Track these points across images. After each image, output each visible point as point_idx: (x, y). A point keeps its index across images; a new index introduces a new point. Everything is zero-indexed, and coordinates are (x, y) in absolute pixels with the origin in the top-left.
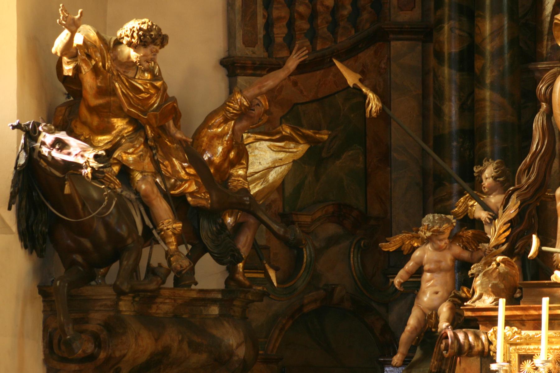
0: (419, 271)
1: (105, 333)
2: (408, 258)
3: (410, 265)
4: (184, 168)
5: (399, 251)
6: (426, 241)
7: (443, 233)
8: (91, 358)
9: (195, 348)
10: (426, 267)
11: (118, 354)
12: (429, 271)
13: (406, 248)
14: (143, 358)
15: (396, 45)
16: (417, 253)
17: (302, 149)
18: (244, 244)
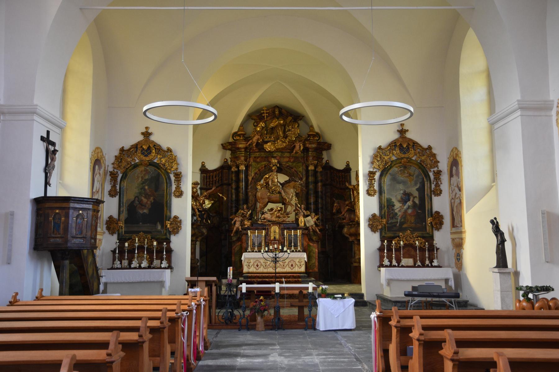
0: (236, 221)
18: (205, 216)
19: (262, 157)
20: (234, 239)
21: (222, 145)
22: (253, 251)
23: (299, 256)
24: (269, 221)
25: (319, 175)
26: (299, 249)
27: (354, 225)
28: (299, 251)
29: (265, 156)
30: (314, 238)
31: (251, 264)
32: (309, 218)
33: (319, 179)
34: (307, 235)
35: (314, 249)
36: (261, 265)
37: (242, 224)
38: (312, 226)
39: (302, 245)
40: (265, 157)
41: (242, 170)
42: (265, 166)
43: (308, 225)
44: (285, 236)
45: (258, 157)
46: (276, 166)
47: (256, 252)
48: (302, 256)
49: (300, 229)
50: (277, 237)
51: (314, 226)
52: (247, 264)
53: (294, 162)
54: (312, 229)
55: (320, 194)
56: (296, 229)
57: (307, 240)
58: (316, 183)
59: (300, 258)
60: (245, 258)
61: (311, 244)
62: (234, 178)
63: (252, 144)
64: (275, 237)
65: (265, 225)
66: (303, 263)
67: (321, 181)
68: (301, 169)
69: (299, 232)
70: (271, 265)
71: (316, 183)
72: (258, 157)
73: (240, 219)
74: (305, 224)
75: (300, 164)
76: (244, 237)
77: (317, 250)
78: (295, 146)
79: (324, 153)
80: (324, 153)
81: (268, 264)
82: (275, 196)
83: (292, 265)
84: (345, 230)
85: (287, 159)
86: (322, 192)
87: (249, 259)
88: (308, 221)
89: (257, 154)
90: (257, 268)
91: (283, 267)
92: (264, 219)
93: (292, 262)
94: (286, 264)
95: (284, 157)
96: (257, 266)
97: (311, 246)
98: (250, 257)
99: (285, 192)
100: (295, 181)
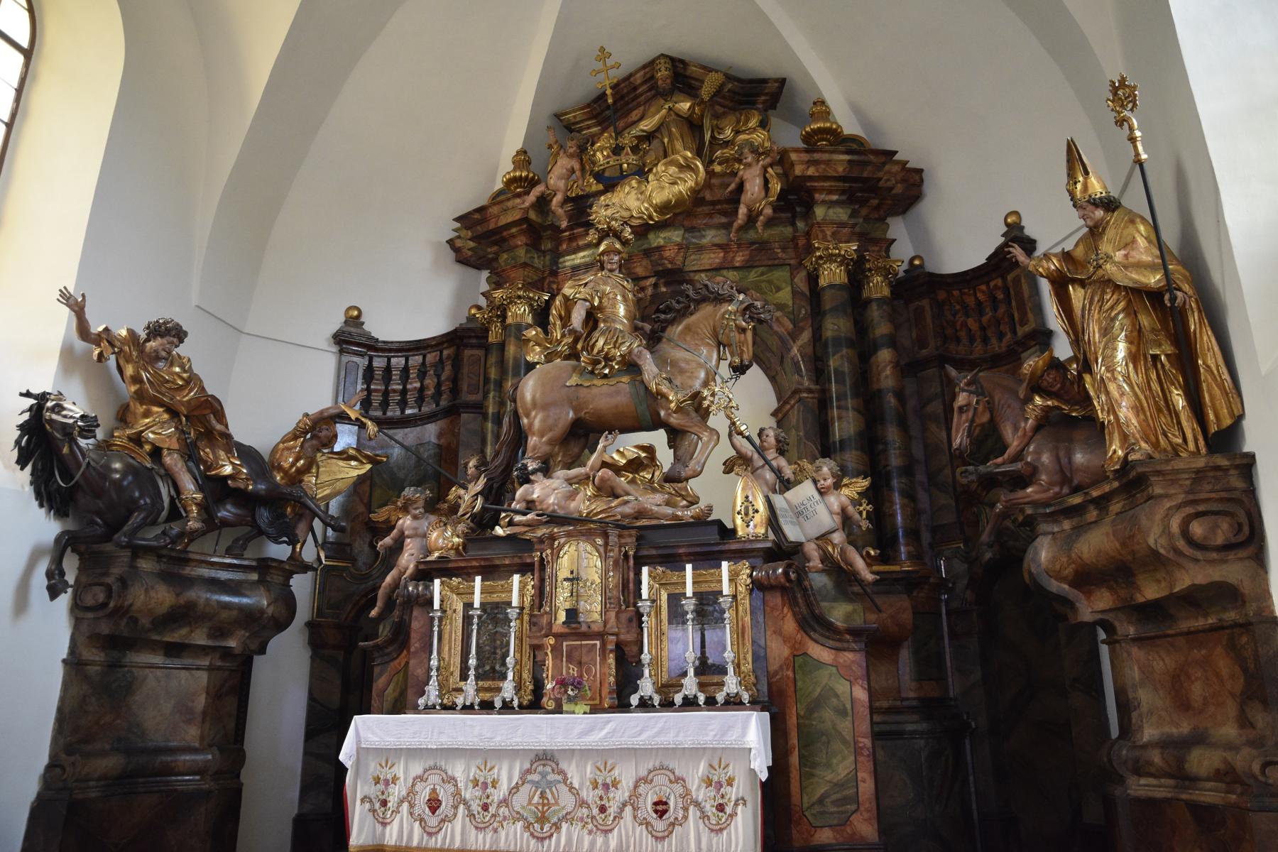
2: (393, 527)
5: (387, 521)
6: (405, 509)
7: (415, 502)
11: (126, 603)
13: (393, 518)
14: (163, 609)
15: (464, 416)
16: (401, 522)
17: (369, 466)
20: (384, 631)
21: (450, 242)
24: (555, 519)
25: (875, 313)
26: (731, 684)
27: (1102, 503)
30: (839, 613)
31: (396, 792)
32: (805, 492)
33: (882, 329)
34: (782, 589)
35: (842, 687)
36: (459, 800)
38: (824, 537)
43: (792, 533)
44: (644, 606)
46: (618, 235)
48: (731, 739)
50: (592, 609)
51: (838, 537)
53: (747, 267)
54: (826, 557)
55: (891, 400)
56: (707, 558)
57: (790, 625)
58: (863, 346)
59: (720, 757)
60: (362, 752)
61: (819, 652)
63: (543, 203)
65: (528, 545)
67: (892, 342)
68: (785, 295)
69: (729, 578)
70: (519, 801)
71: (863, 346)
74: (773, 521)
75: (781, 275)
76: (416, 625)
77: (861, 694)
79: (897, 228)
80: (897, 228)
82: (609, 395)
83: (661, 808)
84: (1043, 553)
85: (715, 258)
86: (900, 395)
87: (389, 755)
88: (799, 513)
90: (433, 821)
92: (530, 505)
93: (660, 779)
94: (621, 794)
95: (700, 249)
97: (819, 664)
98: (390, 741)
99: (661, 362)
100: (719, 299)
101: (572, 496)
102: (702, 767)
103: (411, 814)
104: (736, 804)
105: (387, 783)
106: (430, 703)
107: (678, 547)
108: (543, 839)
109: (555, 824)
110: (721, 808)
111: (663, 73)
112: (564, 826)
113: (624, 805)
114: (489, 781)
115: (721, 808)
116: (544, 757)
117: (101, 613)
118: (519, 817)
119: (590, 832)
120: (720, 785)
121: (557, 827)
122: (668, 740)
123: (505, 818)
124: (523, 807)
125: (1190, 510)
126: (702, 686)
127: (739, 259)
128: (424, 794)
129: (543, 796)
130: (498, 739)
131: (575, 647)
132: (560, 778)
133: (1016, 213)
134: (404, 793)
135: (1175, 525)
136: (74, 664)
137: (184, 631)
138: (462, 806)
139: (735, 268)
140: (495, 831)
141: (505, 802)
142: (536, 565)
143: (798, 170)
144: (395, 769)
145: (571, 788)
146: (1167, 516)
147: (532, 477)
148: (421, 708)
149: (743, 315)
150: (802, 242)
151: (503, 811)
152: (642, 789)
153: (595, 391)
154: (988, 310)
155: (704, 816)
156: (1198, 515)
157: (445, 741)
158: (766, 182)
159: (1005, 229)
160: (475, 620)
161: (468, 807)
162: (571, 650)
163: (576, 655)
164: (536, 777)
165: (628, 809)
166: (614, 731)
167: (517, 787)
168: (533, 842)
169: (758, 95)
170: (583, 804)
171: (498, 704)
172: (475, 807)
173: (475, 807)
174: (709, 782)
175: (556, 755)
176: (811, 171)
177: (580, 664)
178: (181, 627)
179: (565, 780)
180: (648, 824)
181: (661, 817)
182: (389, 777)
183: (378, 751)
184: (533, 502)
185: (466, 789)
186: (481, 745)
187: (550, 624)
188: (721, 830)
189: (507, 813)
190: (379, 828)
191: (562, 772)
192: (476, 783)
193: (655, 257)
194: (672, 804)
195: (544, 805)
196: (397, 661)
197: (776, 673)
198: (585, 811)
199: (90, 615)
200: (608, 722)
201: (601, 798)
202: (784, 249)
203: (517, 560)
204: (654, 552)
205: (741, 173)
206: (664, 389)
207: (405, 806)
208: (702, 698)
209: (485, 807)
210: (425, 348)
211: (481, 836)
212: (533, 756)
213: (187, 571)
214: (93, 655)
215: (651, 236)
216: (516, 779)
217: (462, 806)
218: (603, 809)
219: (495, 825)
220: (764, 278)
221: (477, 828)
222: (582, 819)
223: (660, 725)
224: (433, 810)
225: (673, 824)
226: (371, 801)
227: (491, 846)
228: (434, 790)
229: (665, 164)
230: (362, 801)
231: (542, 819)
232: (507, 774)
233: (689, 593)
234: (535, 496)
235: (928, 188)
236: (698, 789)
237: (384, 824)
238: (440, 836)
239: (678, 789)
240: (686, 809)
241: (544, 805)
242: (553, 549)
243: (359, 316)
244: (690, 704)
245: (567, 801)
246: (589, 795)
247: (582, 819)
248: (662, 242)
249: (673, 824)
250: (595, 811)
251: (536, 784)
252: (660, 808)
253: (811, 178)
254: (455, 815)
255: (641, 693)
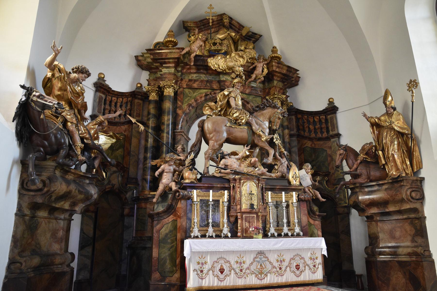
1: (48, 180)
2: (159, 168)
3: (160, 170)
4: (84, 130)
5: (156, 165)
6: (166, 162)
8: (40, 190)
9: (80, 192)
10: (166, 171)
11: (52, 189)
12: (166, 172)
13: (158, 165)
14: (62, 193)
16: (162, 167)
17: (114, 140)
19: (202, 81)
22: (204, 236)
23: (311, 245)
24: (236, 173)
28: (298, 235)
29: (206, 79)
31: (206, 268)
36: (231, 268)
37: (179, 177)
39: (300, 223)
40: (207, 81)
41: (169, 96)
42: (206, 95)
45: (195, 81)
47: (211, 237)
48: (317, 245)
49: (294, 190)
52: (198, 267)
53: (249, 94)
59: (313, 251)
60: (193, 253)
62: (152, 111)
64: (252, 205)
66: (320, 260)
70: (253, 268)
72: (195, 81)
73: (172, 168)
76: (181, 205)
78: (255, 68)
81: (245, 266)
83: (298, 267)
87: (202, 254)
89: (194, 76)
90: (222, 276)
91: (280, 271)
94: (285, 264)
96: (222, 271)
98: (204, 249)
101: (240, 166)
102: (309, 255)
103: (213, 274)
104: (319, 265)
105: (202, 264)
106: (196, 235)
107: (277, 186)
108: (262, 279)
109: (265, 274)
110: (314, 266)
111: (226, 21)
112: (269, 275)
113: (287, 267)
114: (242, 261)
115: (314, 266)
116: (261, 253)
117: (39, 193)
118: (253, 273)
119: (277, 276)
120: (314, 259)
121: (266, 275)
122: (300, 246)
123: (248, 274)
124: (254, 270)
125: (411, 190)
126: (289, 230)
127: (247, 91)
128: (219, 267)
129: (261, 265)
130: (245, 247)
131: (248, 217)
132: (266, 259)
133: (333, 99)
134: (210, 267)
135: (408, 193)
136: (20, 214)
137: (62, 203)
138: (232, 271)
139: (246, 94)
140: (245, 278)
141: (248, 268)
142: (232, 188)
143: (274, 68)
144: (205, 259)
145: (270, 262)
146: (407, 191)
147: (226, 157)
148: (192, 237)
149: (281, 114)
150: (267, 91)
151: (248, 271)
152: (292, 262)
153: (236, 129)
154: (318, 124)
155: (310, 269)
156: (413, 191)
157: (226, 248)
158: (263, 69)
159: (328, 103)
160: (211, 206)
161: (235, 271)
162: (246, 217)
163: (248, 219)
164: (258, 259)
165: (288, 268)
166: (284, 244)
167: (252, 263)
168: (258, 281)
169: (252, 38)
170: (274, 267)
171: (223, 235)
172: (238, 271)
173: (238, 271)
174: (311, 259)
175: (265, 252)
176: (277, 70)
177: (249, 222)
178: (62, 201)
179: (268, 259)
180: (294, 272)
181: (298, 270)
182: (203, 262)
183: (199, 252)
184: (228, 165)
185: (234, 265)
186: (240, 249)
187: (241, 209)
188: (315, 272)
189: (249, 272)
190: (200, 280)
191: (266, 257)
192: (237, 262)
193: (222, 84)
194: (301, 265)
195: (261, 269)
196: (167, 219)
197: (304, 227)
198: (275, 270)
199: (32, 193)
200: (282, 241)
201: (280, 265)
202: (261, 91)
203: (222, 186)
204: (269, 187)
205: (256, 64)
206: (261, 133)
207: (211, 272)
208: (290, 234)
209: (241, 270)
210: (123, 96)
211: (240, 280)
212: (257, 253)
213: (67, 177)
214: (27, 212)
215: (221, 76)
216: (252, 260)
217: (232, 271)
218: (280, 269)
219: (245, 276)
220: (254, 99)
221: (238, 278)
222: (274, 272)
223: (297, 242)
224: (222, 273)
225: (301, 272)
226: (197, 271)
227: (244, 283)
228: (222, 266)
229: (235, 54)
230: (194, 270)
231: (261, 273)
232: (248, 259)
233: (284, 201)
234: (229, 164)
235: (300, 83)
236: (308, 261)
237: (202, 279)
238: (225, 281)
239: (302, 261)
240: (305, 267)
241: (261, 269)
242: (240, 183)
243: (104, 78)
244: (286, 235)
245: (269, 267)
246: (276, 264)
247: (274, 272)
248: (224, 79)
249: (301, 272)
250: (278, 269)
251: (259, 262)
252: (297, 267)
253: (276, 72)
254: (230, 274)
255: (271, 232)
